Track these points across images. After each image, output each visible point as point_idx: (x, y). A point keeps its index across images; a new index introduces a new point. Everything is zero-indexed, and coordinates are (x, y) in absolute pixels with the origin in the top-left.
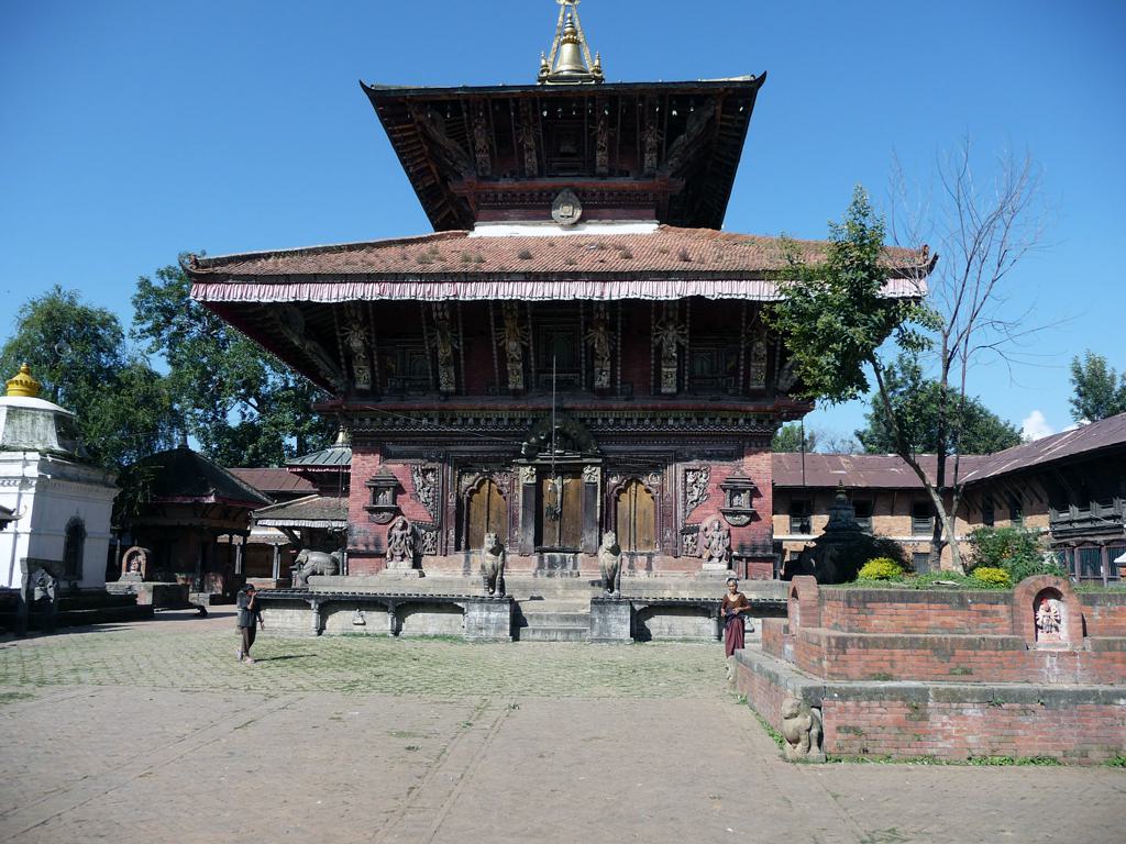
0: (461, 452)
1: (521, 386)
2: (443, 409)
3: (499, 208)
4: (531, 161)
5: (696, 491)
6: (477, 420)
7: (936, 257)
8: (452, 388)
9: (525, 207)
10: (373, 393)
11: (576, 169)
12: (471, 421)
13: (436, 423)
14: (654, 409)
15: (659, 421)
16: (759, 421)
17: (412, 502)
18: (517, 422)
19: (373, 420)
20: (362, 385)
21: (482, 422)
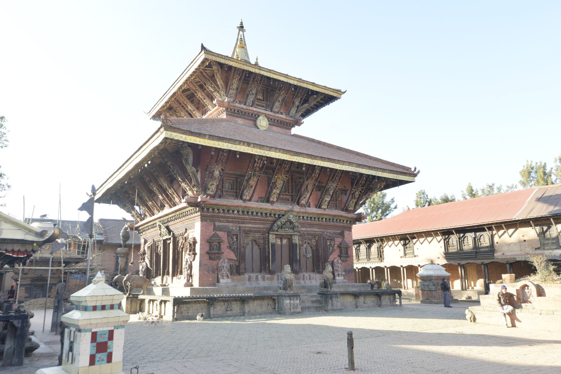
0: (246, 227)
1: (275, 200)
2: (245, 207)
3: (234, 116)
4: (251, 98)
5: (331, 248)
6: (257, 213)
7: (419, 172)
8: (248, 198)
9: (244, 118)
10: (213, 197)
11: (263, 107)
12: (255, 213)
13: (241, 213)
14: (321, 214)
15: (320, 219)
16: (350, 222)
17: (228, 250)
18: (273, 215)
19: (213, 209)
20: (209, 192)
21: (259, 214)
